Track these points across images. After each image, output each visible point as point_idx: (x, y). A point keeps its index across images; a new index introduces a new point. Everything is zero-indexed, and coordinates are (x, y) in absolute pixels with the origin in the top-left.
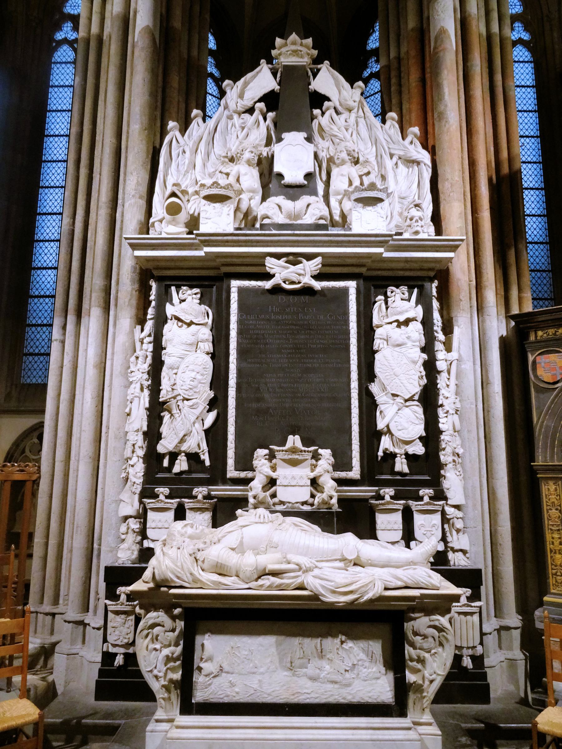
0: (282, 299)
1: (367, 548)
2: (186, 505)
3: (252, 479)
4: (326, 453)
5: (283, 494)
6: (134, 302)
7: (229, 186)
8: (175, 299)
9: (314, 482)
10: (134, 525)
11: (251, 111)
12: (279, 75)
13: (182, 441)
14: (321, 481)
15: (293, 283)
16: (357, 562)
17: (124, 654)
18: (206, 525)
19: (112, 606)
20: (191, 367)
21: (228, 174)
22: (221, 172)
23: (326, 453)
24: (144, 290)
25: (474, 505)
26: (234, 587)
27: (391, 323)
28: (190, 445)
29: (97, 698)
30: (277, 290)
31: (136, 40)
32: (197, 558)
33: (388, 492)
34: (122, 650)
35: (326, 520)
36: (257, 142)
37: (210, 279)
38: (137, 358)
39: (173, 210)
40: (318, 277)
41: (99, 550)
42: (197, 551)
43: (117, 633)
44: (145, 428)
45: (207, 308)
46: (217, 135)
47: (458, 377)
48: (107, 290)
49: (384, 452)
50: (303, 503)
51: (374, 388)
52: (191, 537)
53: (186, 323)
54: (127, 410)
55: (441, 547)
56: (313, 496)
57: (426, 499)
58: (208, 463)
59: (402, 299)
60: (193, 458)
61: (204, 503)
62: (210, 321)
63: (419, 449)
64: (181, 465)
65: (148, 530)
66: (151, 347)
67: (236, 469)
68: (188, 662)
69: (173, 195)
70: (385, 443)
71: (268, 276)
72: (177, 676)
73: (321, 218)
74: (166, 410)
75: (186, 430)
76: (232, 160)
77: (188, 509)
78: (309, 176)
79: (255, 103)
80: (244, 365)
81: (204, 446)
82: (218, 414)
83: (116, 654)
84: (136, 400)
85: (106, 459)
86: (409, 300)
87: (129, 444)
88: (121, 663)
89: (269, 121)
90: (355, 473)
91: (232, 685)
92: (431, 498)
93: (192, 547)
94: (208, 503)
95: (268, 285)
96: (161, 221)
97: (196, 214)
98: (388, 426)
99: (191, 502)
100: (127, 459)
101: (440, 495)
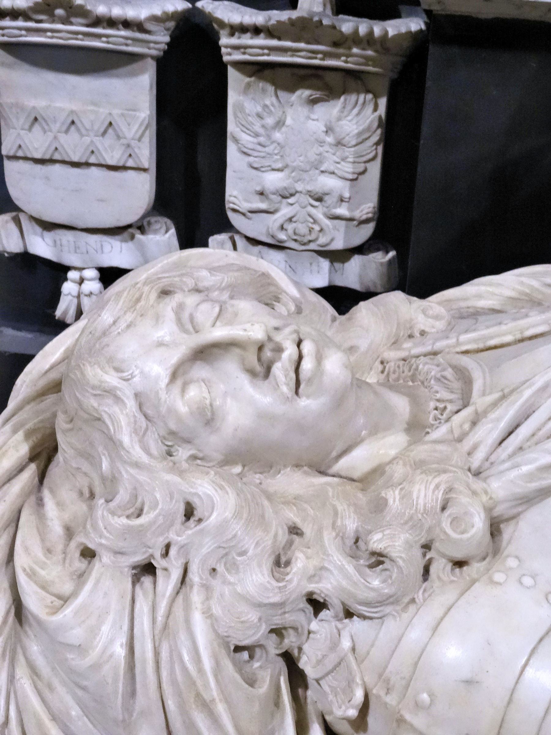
2: (224, 40)
18: (348, 169)
32: (306, 664)
42: (300, 616)
52: (251, 457)
61: (341, 42)
65: (8, 165)
77: (240, 65)
93: (256, 579)
94: (369, 40)
99: (256, 30)
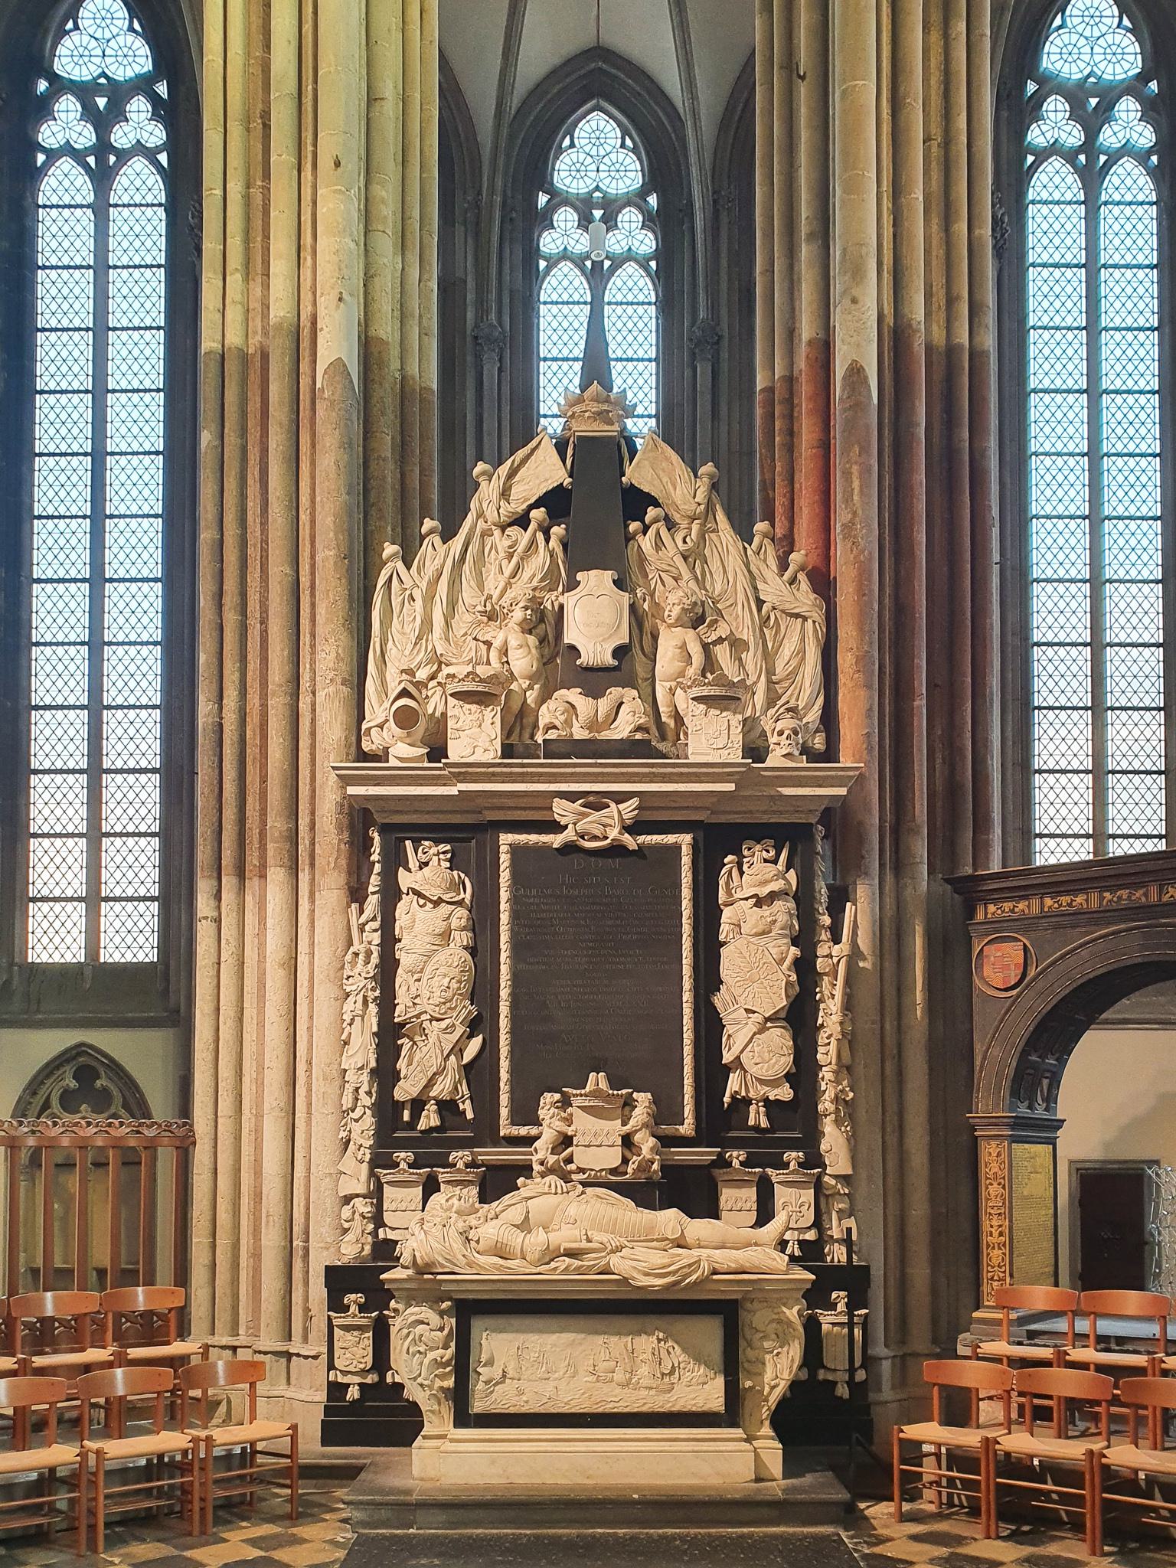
0: (579, 864)
1: (700, 1228)
3: (537, 1138)
4: (643, 1099)
5: (583, 1157)
6: (343, 862)
7: (493, 679)
8: (413, 864)
9: (627, 1141)
10: (363, 1206)
11: (522, 521)
12: (570, 452)
13: (430, 1084)
14: (637, 1138)
15: (595, 838)
16: (682, 1243)
17: (359, 1384)
19: (339, 1320)
20: (442, 970)
21: (488, 644)
22: (475, 639)
23: (643, 1099)
24: (359, 847)
25: (870, 1178)
26: (520, 1269)
27: (746, 899)
28: (442, 1089)
29: (325, 1442)
30: (569, 848)
31: (319, 385)
33: (737, 1156)
34: (357, 1379)
35: (645, 1193)
36: (535, 583)
37: (466, 833)
38: (356, 955)
39: (405, 719)
40: (634, 828)
41: (306, 1250)
43: (348, 1355)
44: (373, 1064)
45: (462, 875)
46: (466, 567)
47: (848, 982)
48: (293, 837)
49: (733, 1097)
50: (613, 1171)
51: (717, 1001)
53: (431, 901)
54: (343, 1037)
55: (811, 1236)
56: (625, 1161)
57: (793, 1165)
58: (470, 1115)
59: (766, 861)
60: (447, 1107)
62: (468, 897)
63: (785, 1093)
64: (430, 1118)
66: (376, 938)
67: (513, 1124)
68: (462, 1365)
69: (404, 693)
70: (734, 1083)
71: (557, 827)
72: (450, 1383)
73: (639, 729)
74: (404, 1036)
75: (429, 1066)
76: (491, 616)
78: (620, 652)
79: (531, 507)
80: (520, 966)
81: (464, 1088)
82: (484, 1039)
83: (348, 1385)
84: (358, 1020)
85: (309, 1112)
86: (775, 862)
87: (349, 1089)
88: (356, 1396)
89: (553, 543)
90: (687, 1128)
91: (521, 1392)
92: (800, 1165)
95: (557, 840)
96: (381, 726)
97: (438, 714)
98: (738, 1057)
100: (346, 1112)
101: (814, 1160)
